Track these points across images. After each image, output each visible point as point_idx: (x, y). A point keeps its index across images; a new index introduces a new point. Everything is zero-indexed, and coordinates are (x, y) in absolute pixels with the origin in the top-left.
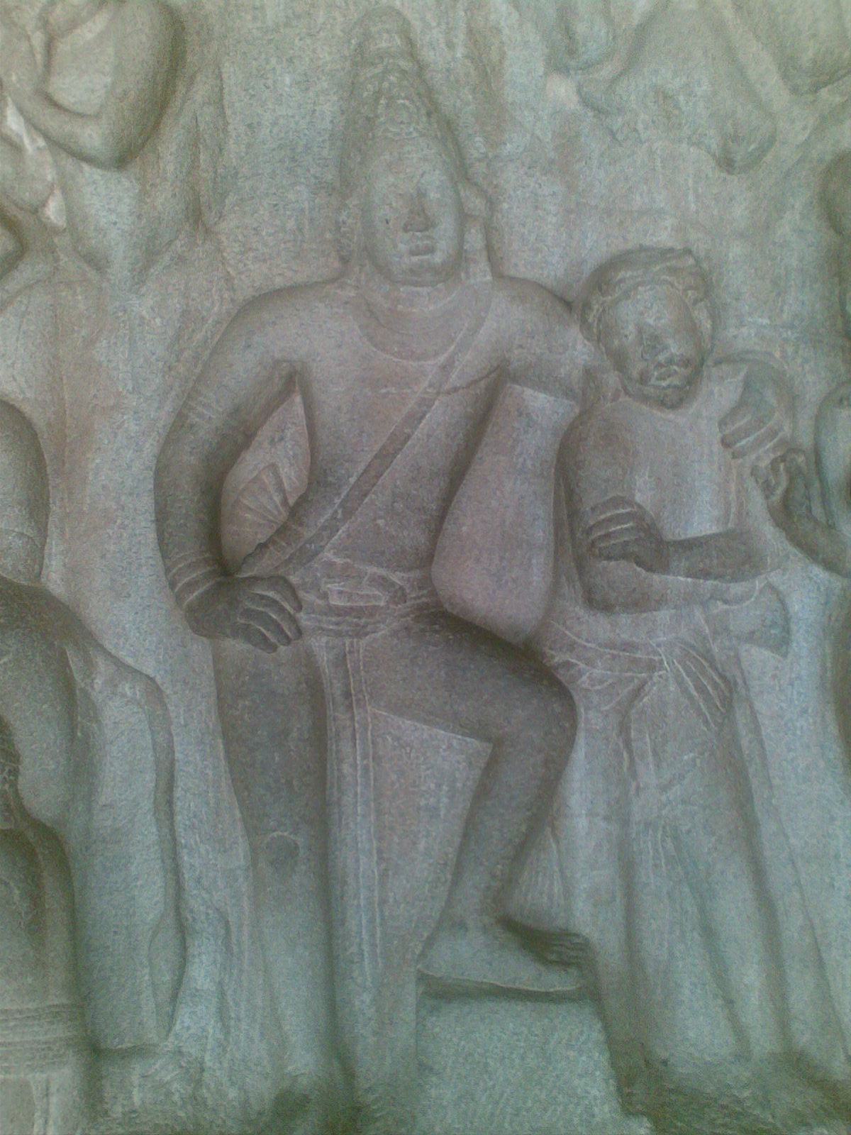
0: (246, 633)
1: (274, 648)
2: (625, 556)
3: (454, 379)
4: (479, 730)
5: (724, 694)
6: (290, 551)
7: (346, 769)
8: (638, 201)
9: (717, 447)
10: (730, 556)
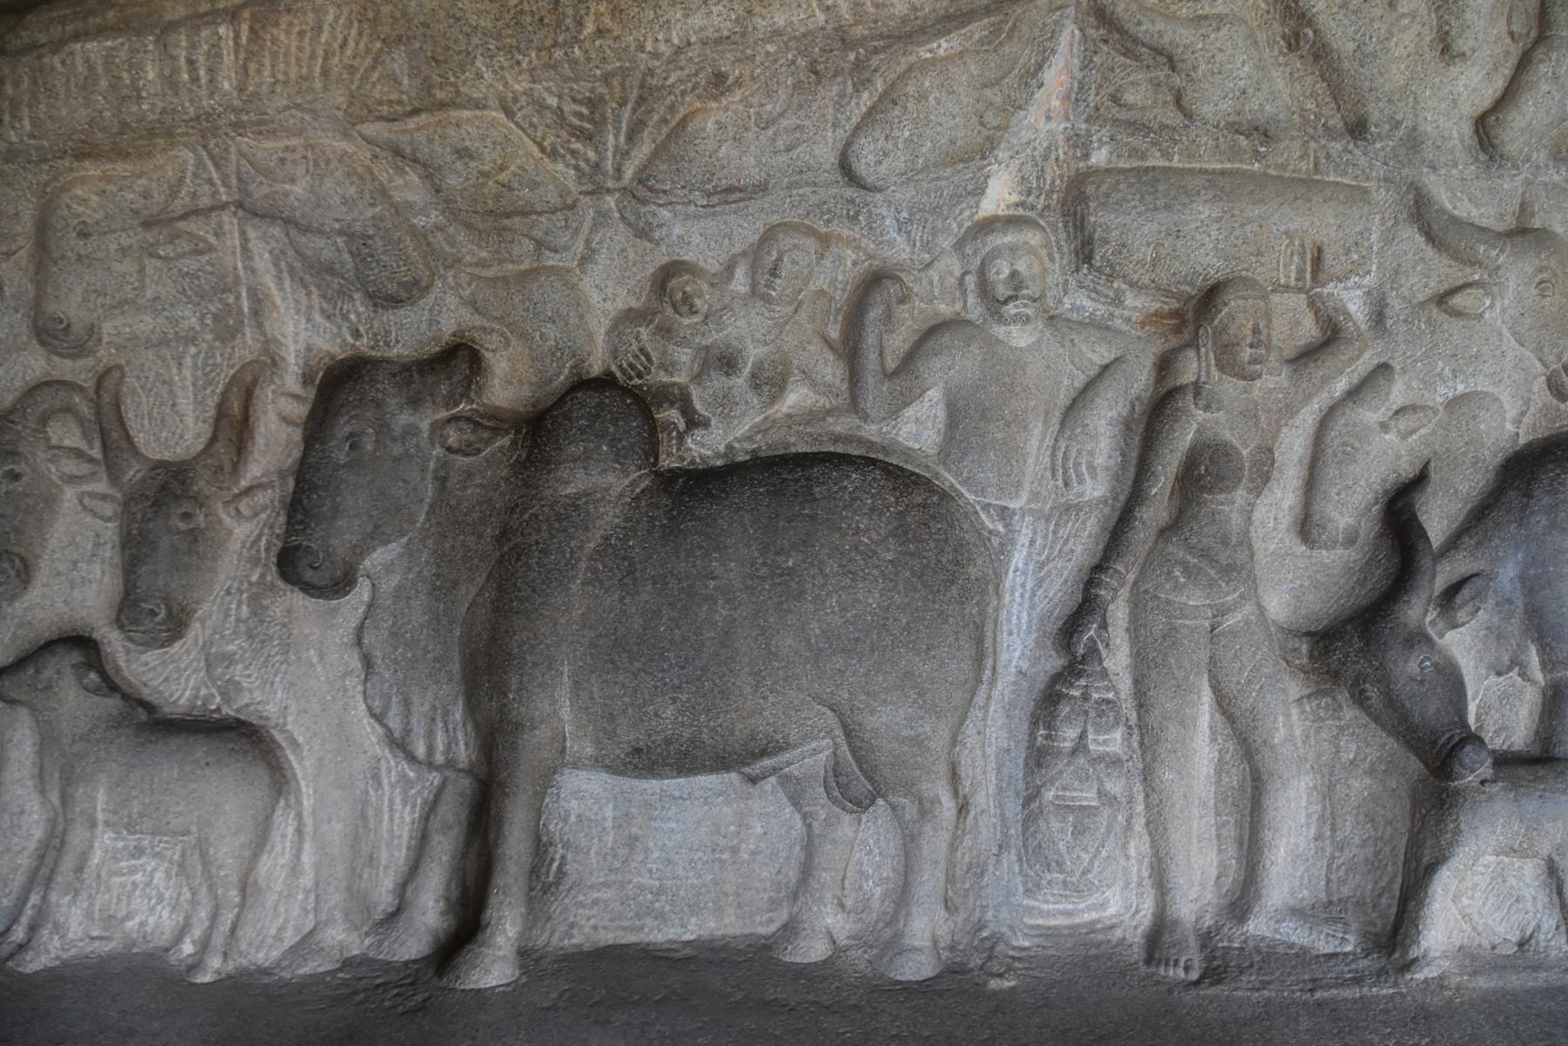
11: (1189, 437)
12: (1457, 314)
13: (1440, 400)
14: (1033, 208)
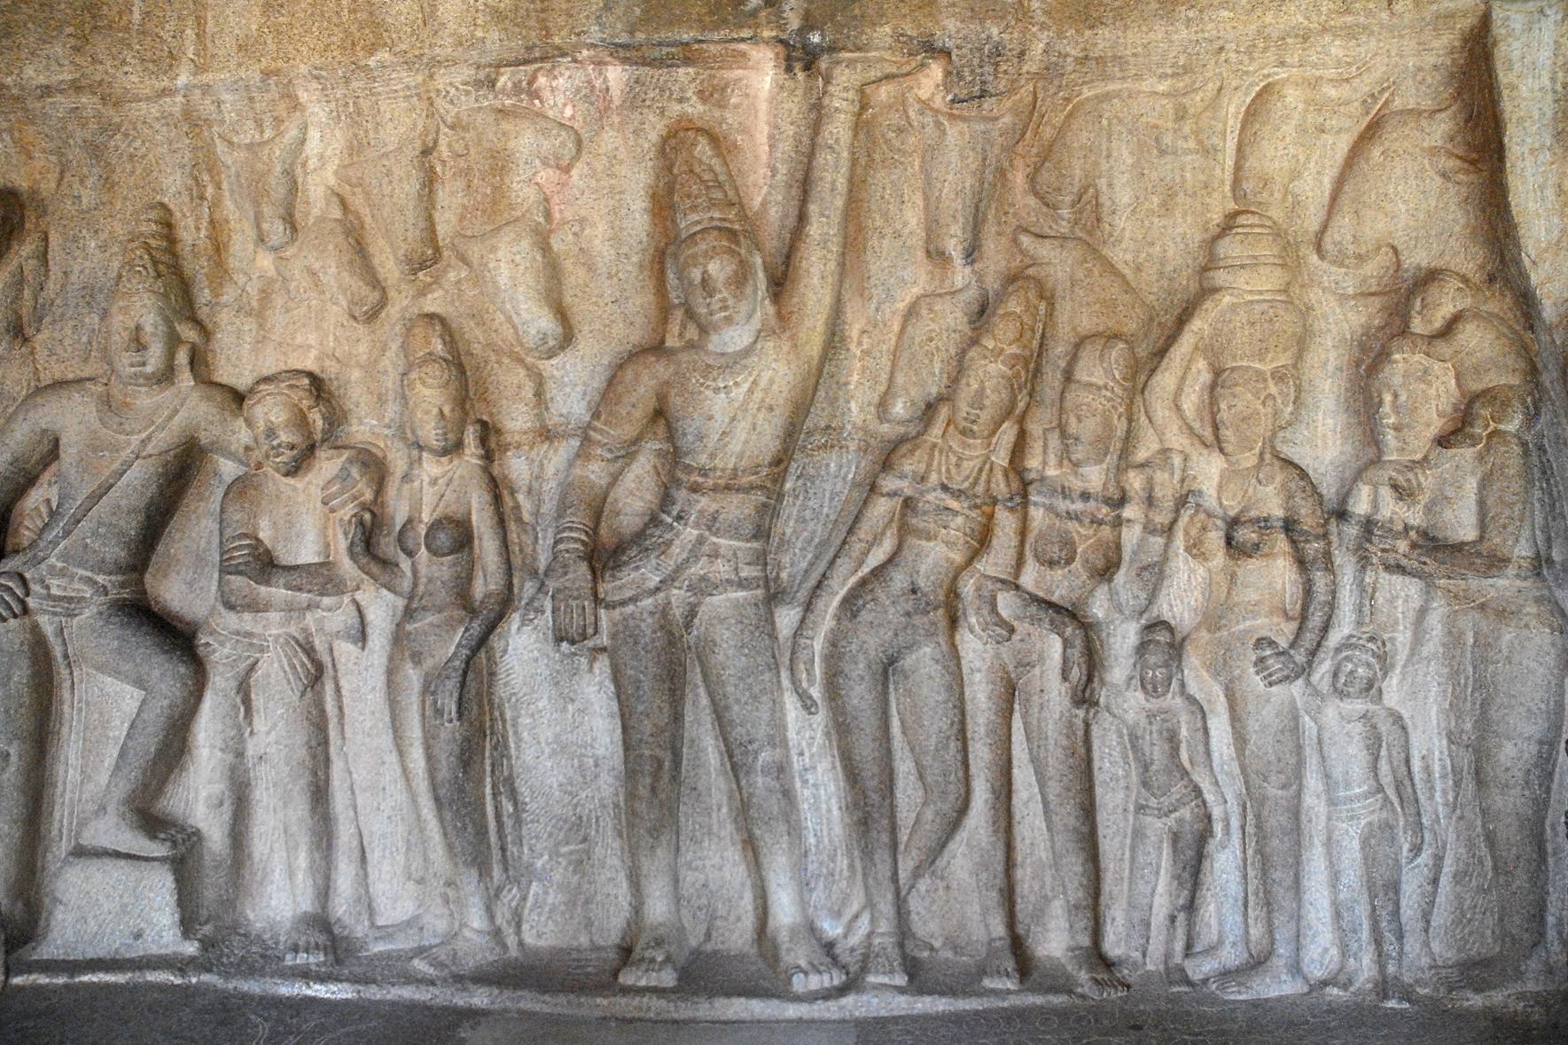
2: (240, 573)
3: (150, 449)
4: (139, 683)
5: (316, 673)
7: (66, 708)
8: (299, 339)
9: (319, 504)
10: (322, 577)
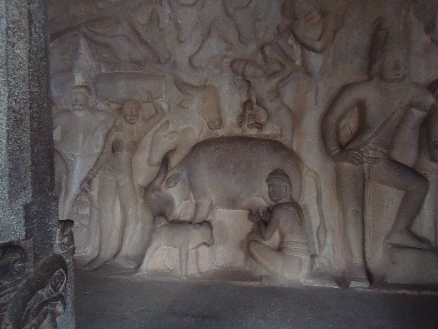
0: (352, 162)
1: (358, 165)
6: (360, 143)
11: (114, 138)
12: (183, 107)
13: (181, 129)
14: (88, 83)
